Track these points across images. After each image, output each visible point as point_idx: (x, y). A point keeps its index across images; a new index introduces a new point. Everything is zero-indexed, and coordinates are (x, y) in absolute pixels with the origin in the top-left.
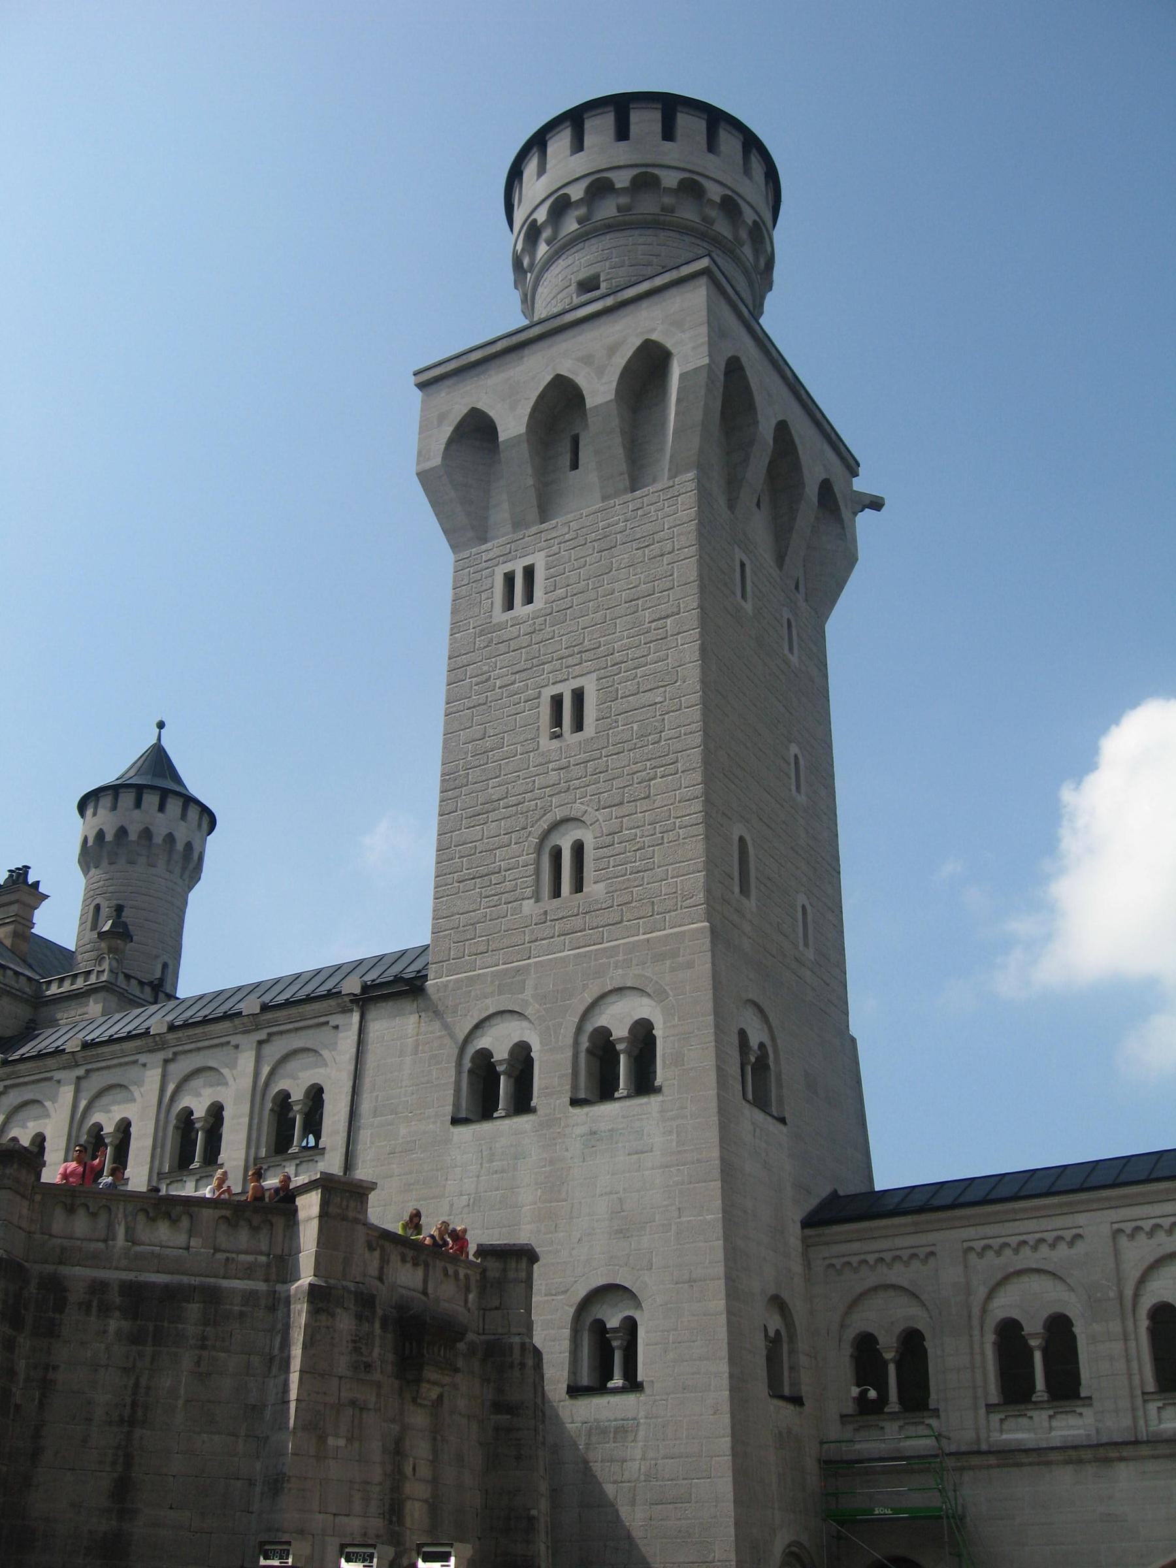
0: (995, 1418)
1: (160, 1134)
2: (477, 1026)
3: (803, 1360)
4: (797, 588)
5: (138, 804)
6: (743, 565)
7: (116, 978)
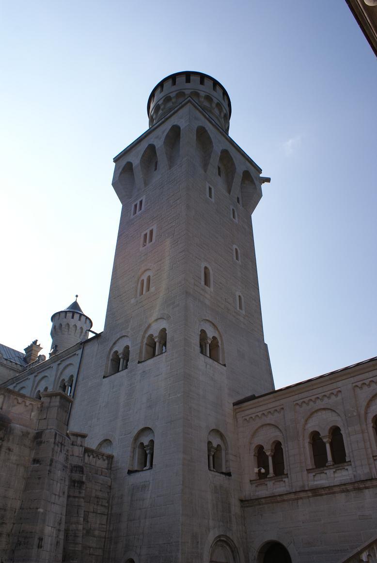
0: (311, 475)
2: (115, 344)
3: (231, 457)
4: (238, 201)
6: (210, 189)
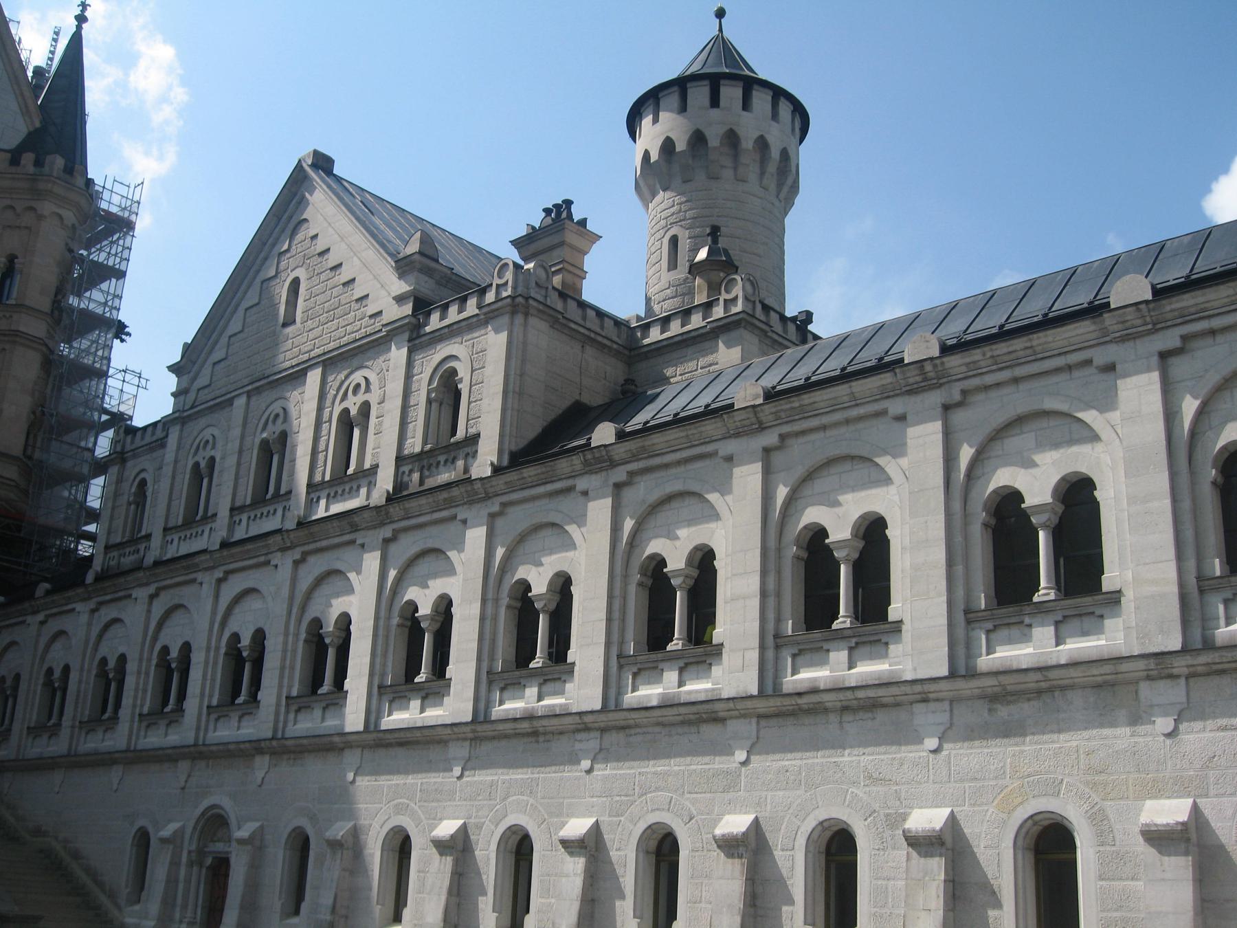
1: (959, 539)
5: (715, 102)
7: (754, 308)
